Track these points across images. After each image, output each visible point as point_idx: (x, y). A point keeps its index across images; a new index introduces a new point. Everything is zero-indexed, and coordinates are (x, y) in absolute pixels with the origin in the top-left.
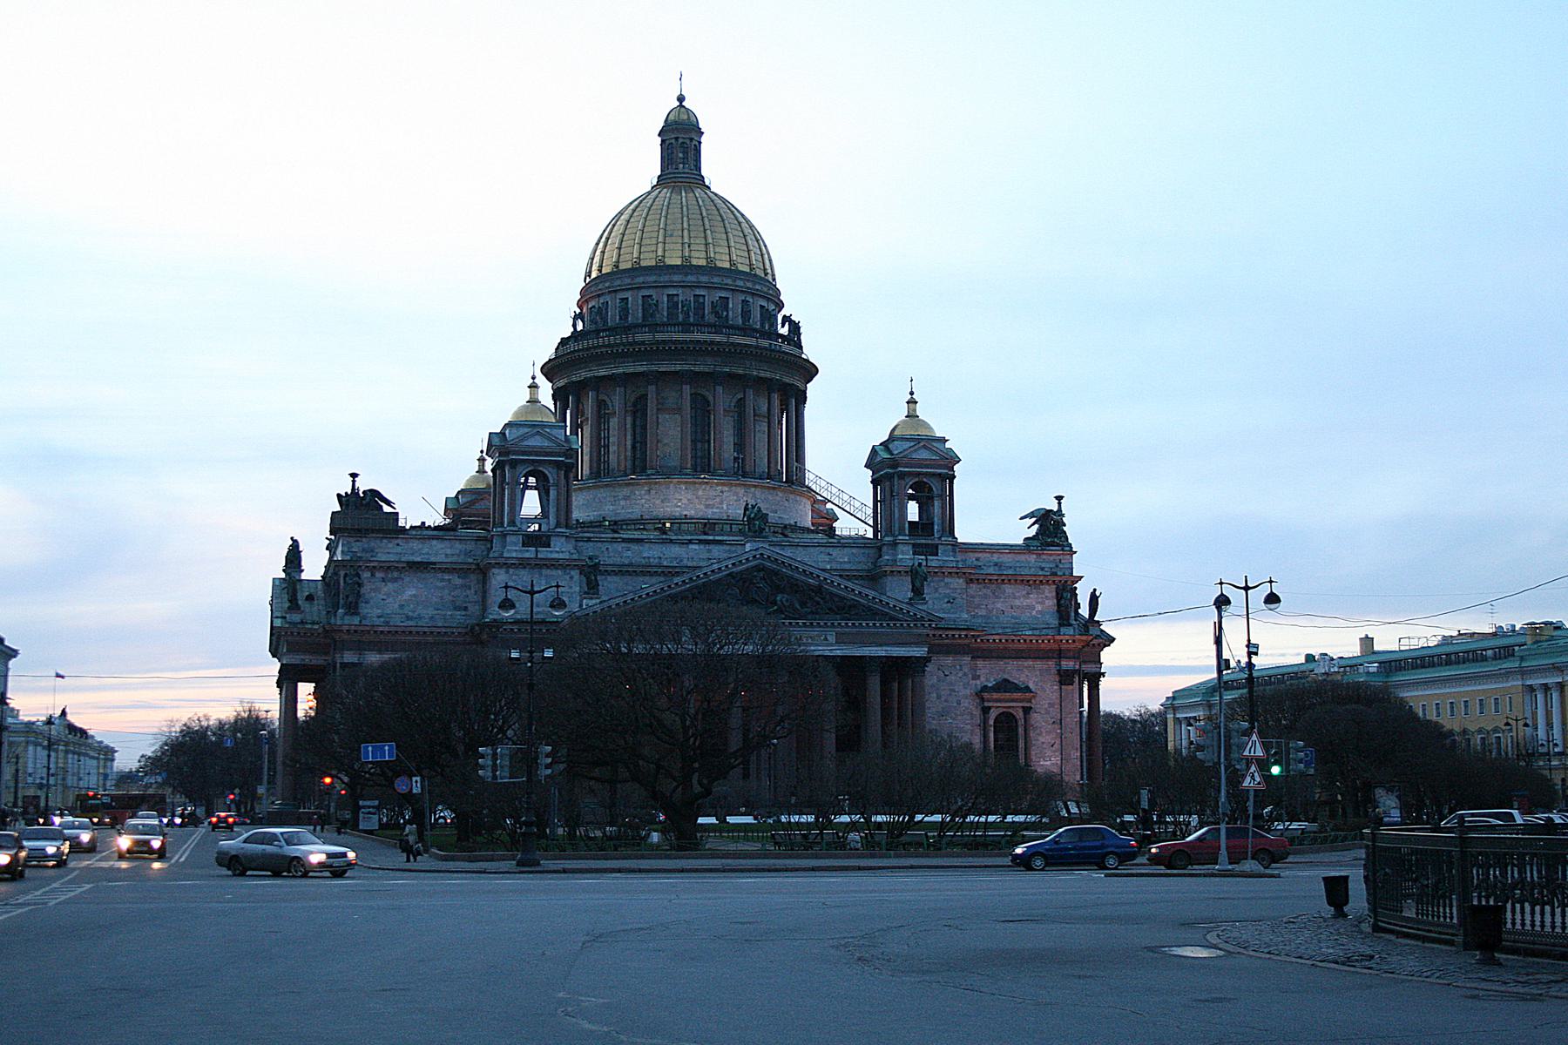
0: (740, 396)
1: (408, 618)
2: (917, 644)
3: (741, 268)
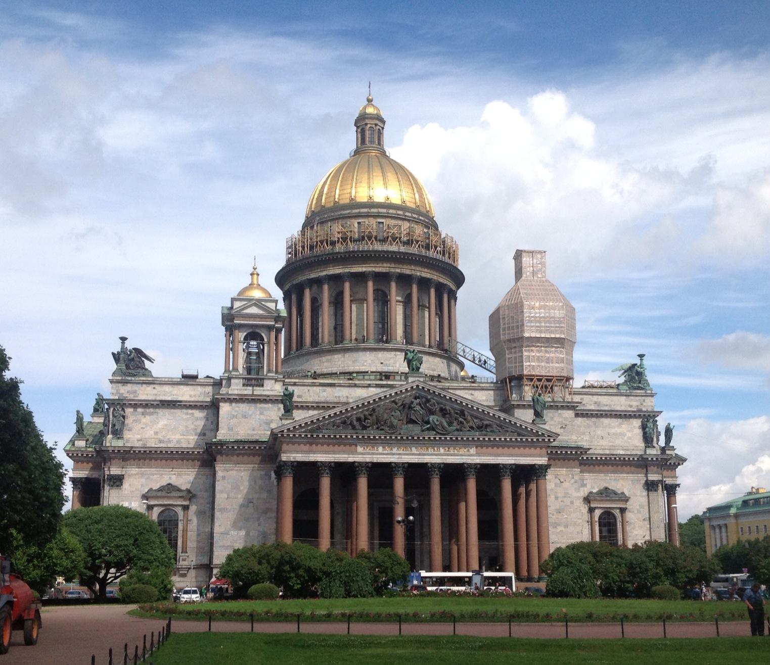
0: (408, 292)
1: (161, 441)
2: (540, 456)
3: (408, 204)
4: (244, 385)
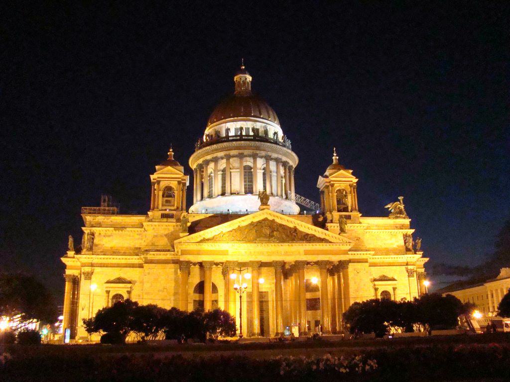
0: (265, 166)
4: (162, 217)
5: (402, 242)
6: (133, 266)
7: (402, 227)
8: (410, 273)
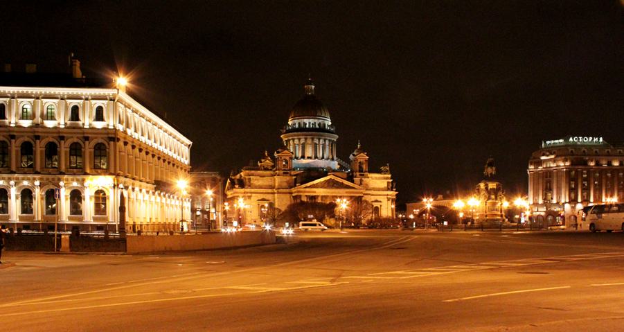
5: (386, 185)
6: (268, 193)
7: (387, 178)
8: (388, 199)
